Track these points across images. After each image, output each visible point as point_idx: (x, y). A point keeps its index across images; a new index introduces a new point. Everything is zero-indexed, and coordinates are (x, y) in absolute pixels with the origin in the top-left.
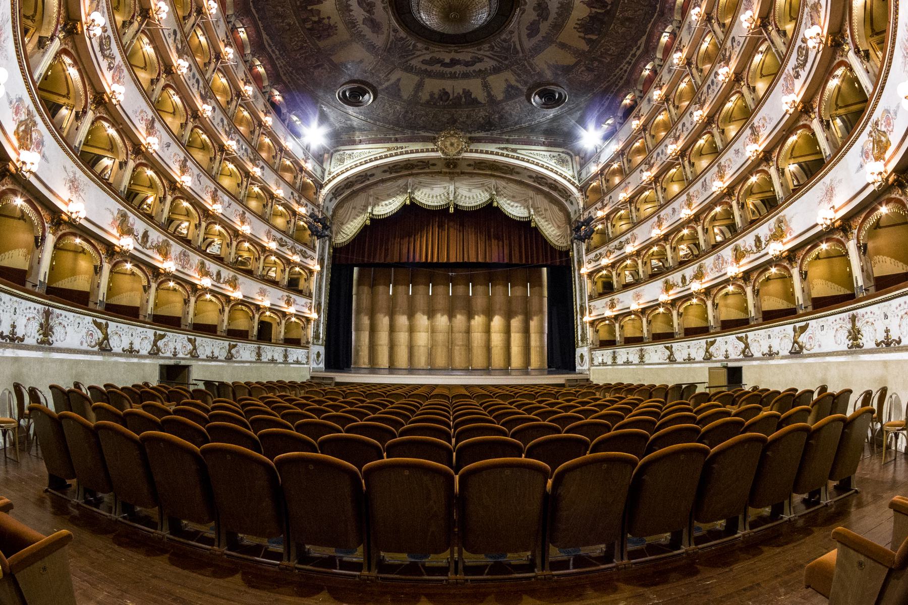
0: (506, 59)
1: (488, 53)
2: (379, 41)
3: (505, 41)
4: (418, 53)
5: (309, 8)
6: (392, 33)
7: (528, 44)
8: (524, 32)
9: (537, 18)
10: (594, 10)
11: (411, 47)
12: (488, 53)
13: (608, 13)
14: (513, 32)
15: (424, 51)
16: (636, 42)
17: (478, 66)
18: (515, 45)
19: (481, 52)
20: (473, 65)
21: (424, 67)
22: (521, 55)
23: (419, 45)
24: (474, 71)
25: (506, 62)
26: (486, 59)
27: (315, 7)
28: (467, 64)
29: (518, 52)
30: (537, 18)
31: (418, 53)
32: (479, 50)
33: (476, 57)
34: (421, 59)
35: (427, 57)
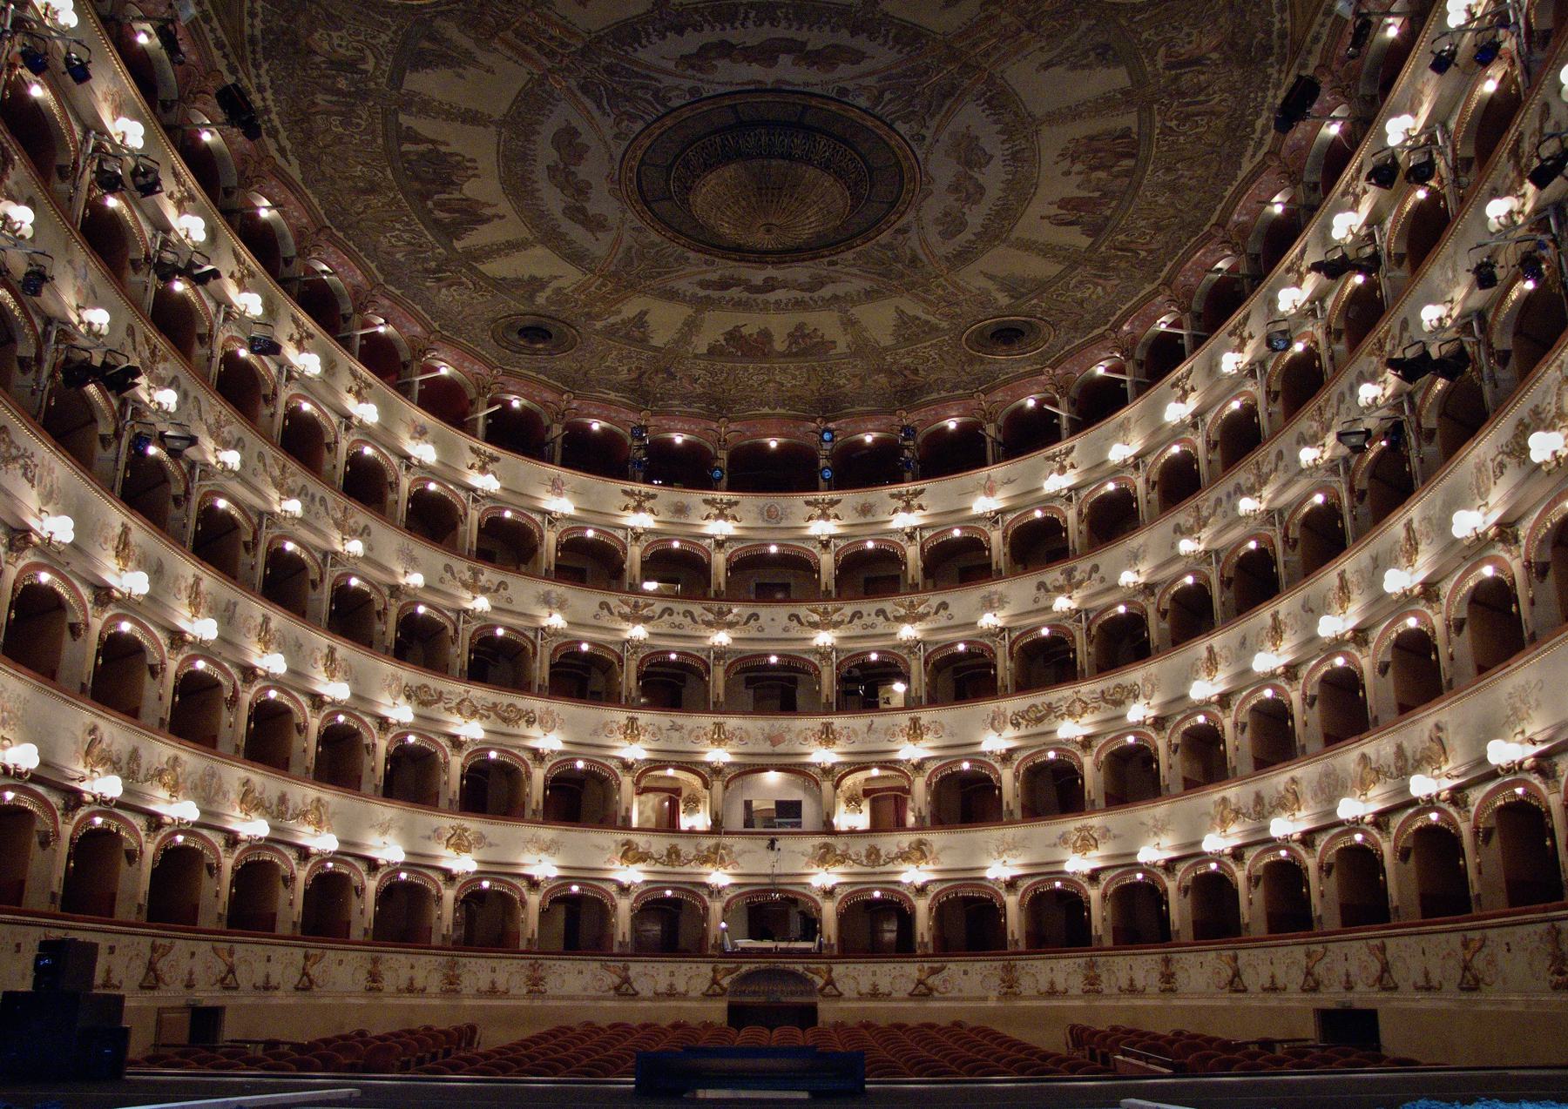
0: (610, 70)
1: (668, 81)
2: (970, 116)
3: (632, 118)
4: (871, 81)
5: (1097, 194)
6: (928, 134)
7: (562, 114)
8: (587, 137)
9: (573, 168)
10: (456, 195)
11: (888, 96)
12: (668, 81)
13: (426, 197)
14: (616, 137)
15: (850, 86)
16: (299, 157)
17: (691, 42)
18: (600, 107)
19: (688, 84)
20: (704, 50)
21: (861, 42)
22: (573, 83)
23: (863, 102)
24: (698, 28)
25: (605, 60)
26: (671, 65)
27: (1085, 194)
28: (725, 49)
29: (584, 89)
30: (573, 168)
31: (871, 81)
32: (694, 91)
33: (701, 70)
34: (865, 66)
35: (844, 70)
